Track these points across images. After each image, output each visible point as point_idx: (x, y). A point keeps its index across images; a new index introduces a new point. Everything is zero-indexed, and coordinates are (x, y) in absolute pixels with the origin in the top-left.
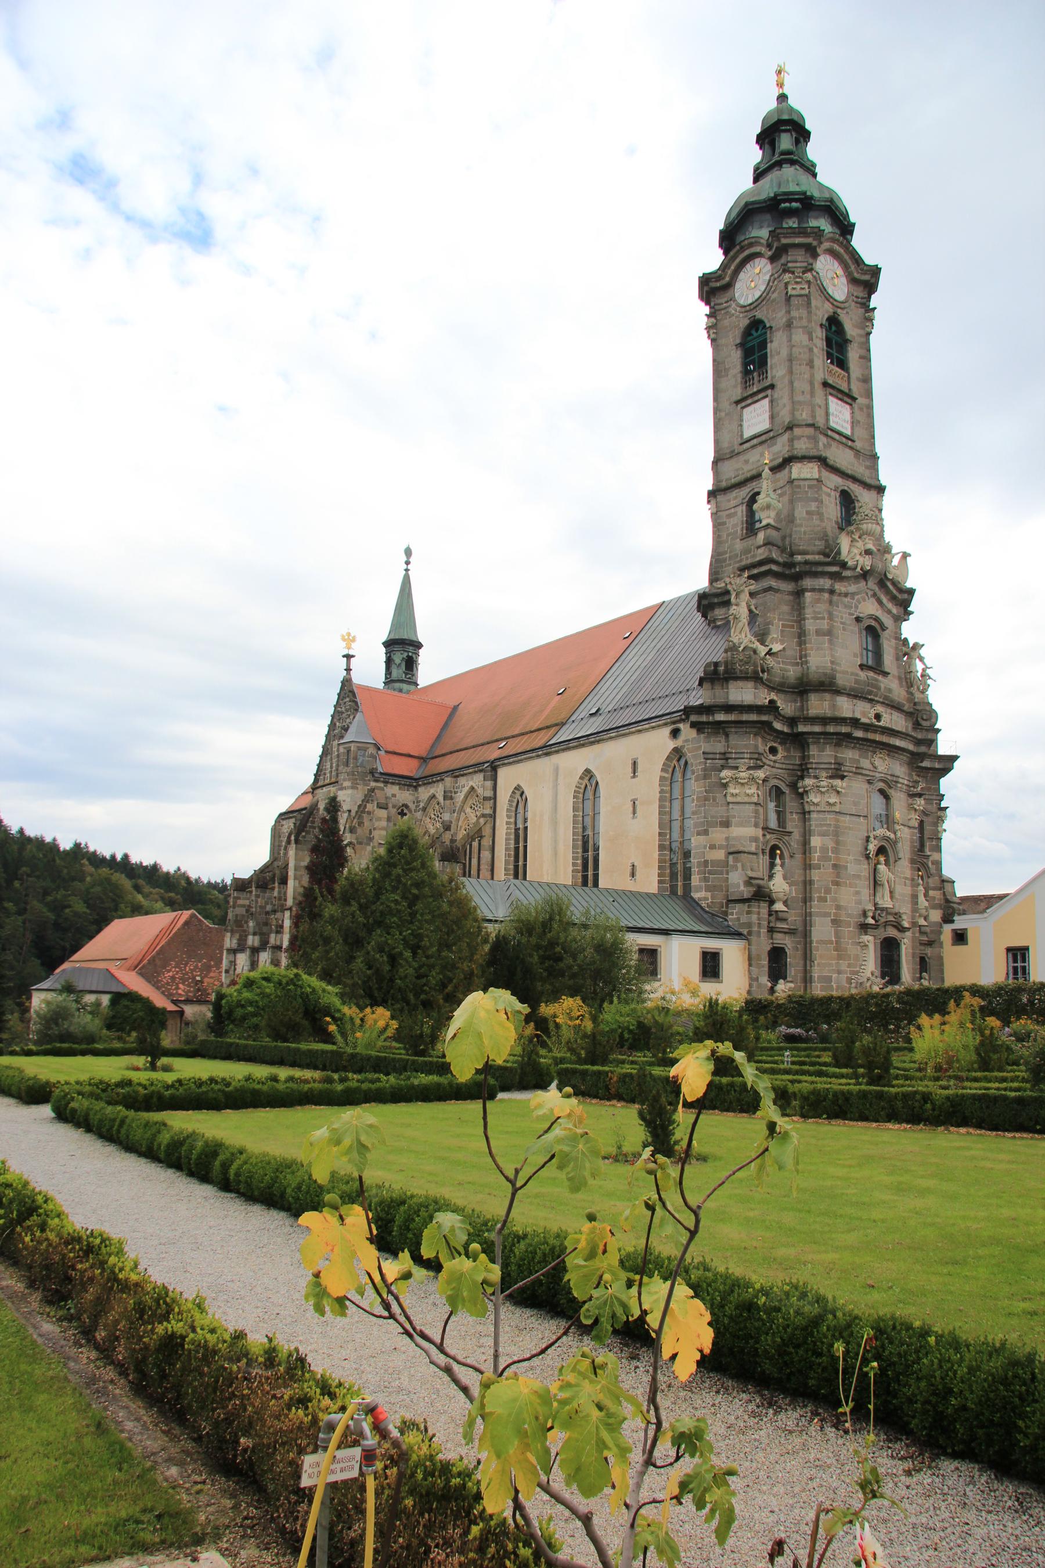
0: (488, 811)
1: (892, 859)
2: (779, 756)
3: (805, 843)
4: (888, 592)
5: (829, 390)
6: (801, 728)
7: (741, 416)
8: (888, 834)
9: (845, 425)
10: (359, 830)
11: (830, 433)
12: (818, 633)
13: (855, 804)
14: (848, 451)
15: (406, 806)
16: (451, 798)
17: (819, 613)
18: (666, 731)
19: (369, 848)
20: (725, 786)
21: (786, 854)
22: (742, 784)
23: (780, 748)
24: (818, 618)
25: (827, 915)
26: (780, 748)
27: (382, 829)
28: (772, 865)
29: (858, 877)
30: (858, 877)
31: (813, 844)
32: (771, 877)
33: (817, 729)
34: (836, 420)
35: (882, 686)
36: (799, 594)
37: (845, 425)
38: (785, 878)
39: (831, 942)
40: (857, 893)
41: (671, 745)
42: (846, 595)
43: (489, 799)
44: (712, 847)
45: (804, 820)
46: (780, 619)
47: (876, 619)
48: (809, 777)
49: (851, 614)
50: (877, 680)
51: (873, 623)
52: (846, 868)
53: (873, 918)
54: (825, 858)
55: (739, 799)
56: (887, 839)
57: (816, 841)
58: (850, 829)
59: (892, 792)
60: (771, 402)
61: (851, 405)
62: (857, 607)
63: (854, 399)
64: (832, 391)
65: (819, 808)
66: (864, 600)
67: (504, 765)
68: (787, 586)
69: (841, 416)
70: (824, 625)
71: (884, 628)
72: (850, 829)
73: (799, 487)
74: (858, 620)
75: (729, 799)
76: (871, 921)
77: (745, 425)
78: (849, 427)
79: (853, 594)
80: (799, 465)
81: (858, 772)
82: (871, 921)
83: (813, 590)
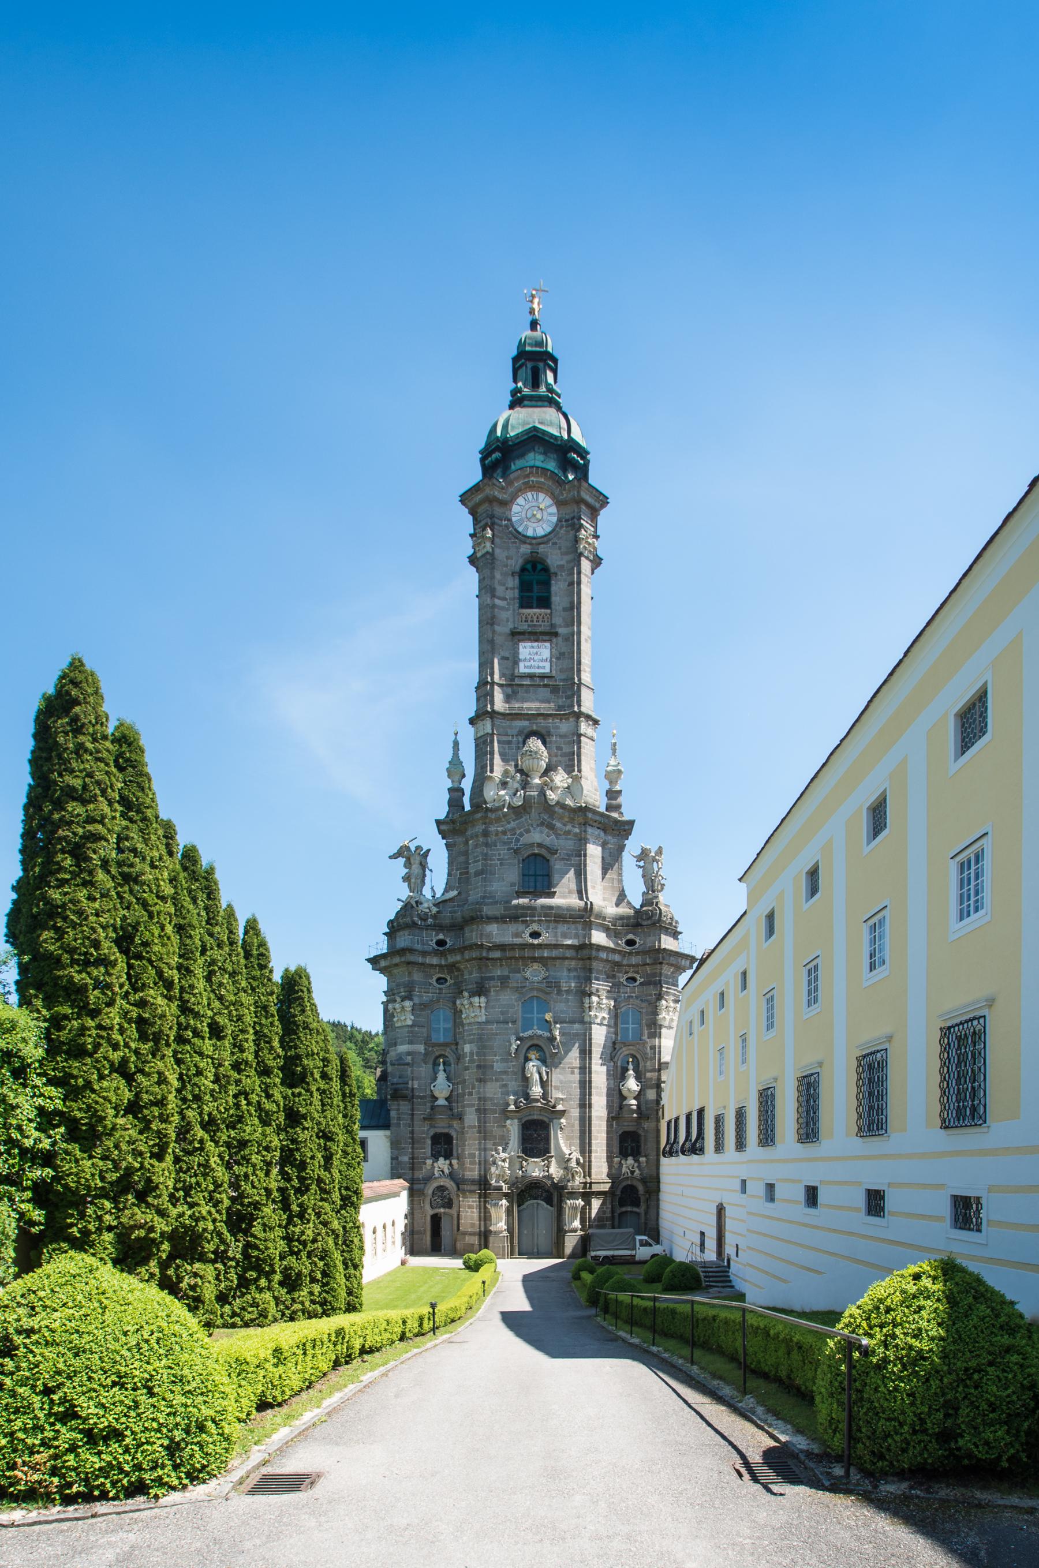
4: (561, 818)
5: (517, 637)
9: (541, 664)
11: (517, 681)
12: (477, 874)
13: (502, 1013)
25: (473, 1105)
29: (505, 1073)
30: (505, 1073)
33: (458, 958)
34: (528, 664)
37: (541, 664)
39: (475, 1127)
52: (492, 1066)
54: (472, 1061)
57: (467, 1048)
58: (497, 1034)
62: (518, 840)
63: (556, 634)
64: (522, 637)
69: (536, 657)
70: (479, 866)
72: (497, 1034)
76: (512, 1107)
83: (472, 838)
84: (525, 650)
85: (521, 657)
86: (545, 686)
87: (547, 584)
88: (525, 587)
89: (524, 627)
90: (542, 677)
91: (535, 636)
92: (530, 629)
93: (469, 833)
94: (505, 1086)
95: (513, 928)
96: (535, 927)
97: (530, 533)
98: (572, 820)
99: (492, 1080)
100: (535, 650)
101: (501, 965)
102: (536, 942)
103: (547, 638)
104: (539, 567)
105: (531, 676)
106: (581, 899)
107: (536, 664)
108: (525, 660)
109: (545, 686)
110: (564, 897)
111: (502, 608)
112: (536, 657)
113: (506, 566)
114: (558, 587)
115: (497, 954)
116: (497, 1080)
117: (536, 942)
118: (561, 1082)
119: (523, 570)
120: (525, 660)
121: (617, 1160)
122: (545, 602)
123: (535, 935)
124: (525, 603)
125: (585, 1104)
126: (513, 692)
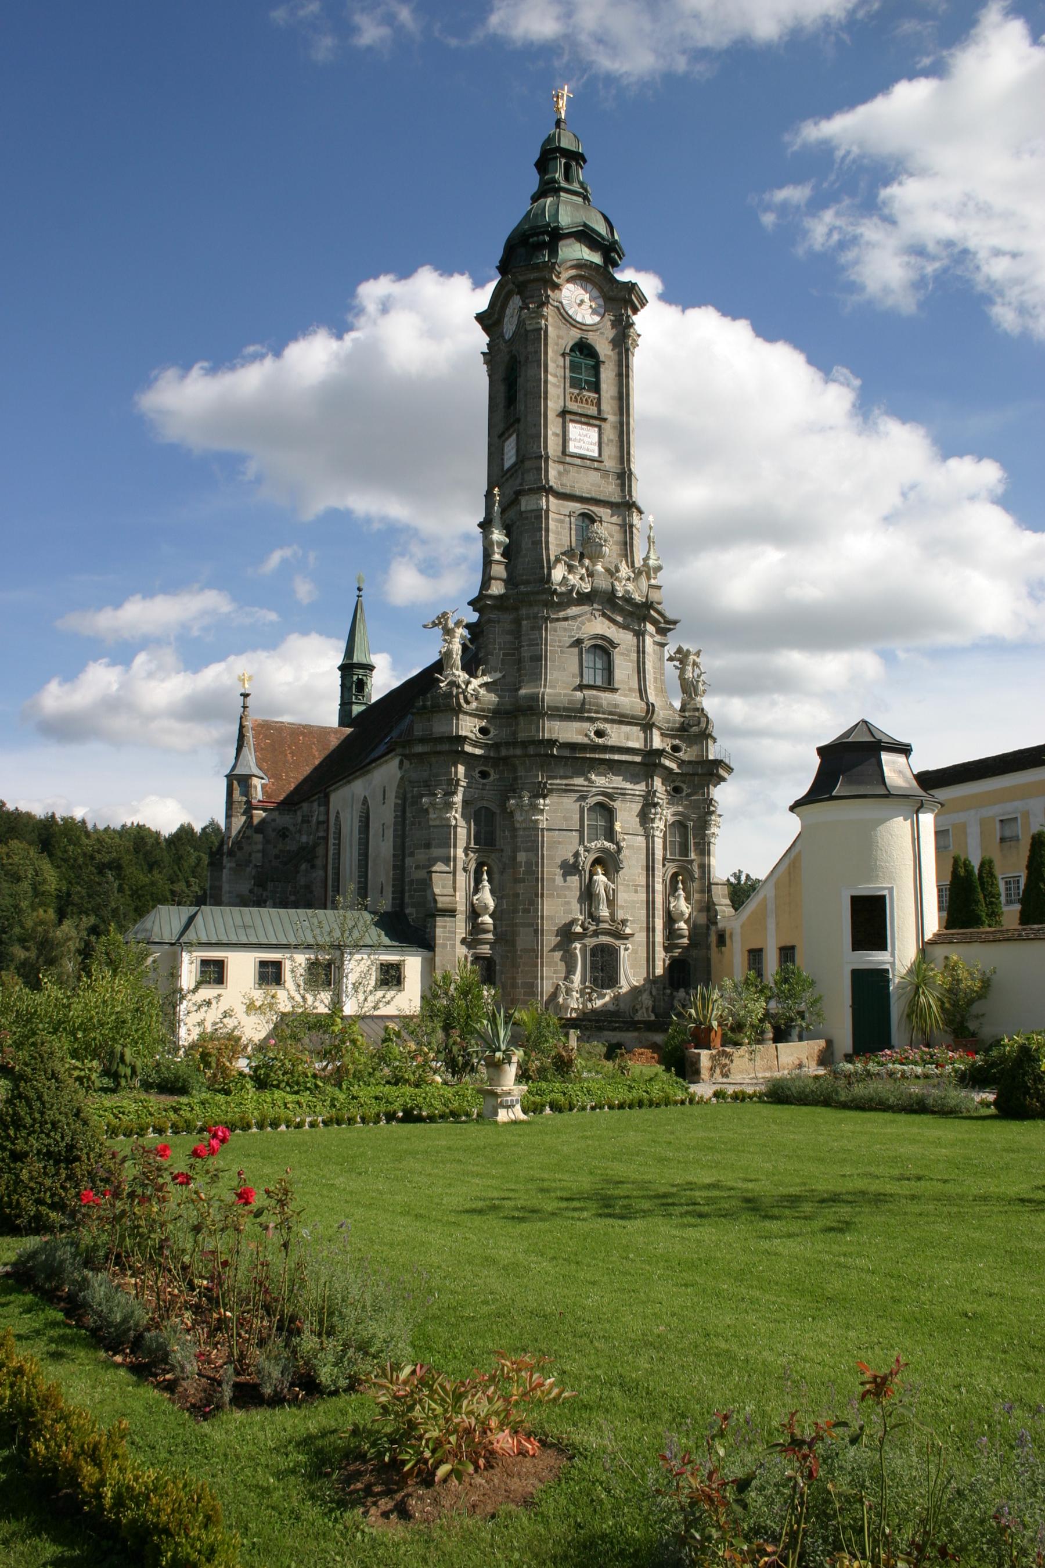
0: (321, 834)
1: (611, 870)
2: (492, 778)
3: (514, 858)
4: (621, 611)
6: (504, 752)
7: (503, 446)
8: (607, 844)
10: (239, 854)
11: (568, 459)
13: (565, 819)
14: (592, 472)
15: (287, 829)
16: (309, 822)
17: (533, 640)
18: (396, 762)
19: (248, 869)
20: (427, 811)
21: (495, 869)
22: (440, 809)
23: (492, 772)
24: (533, 645)
26: (492, 772)
27: (258, 851)
28: (478, 881)
31: (519, 859)
32: (477, 890)
35: (604, 703)
36: (518, 622)
38: (492, 892)
40: (568, 903)
41: (399, 775)
42: (566, 619)
43: (323, 822)
44: (417, 867)
45: (514, 837)
46: (500, 649)
47: (603, 638)
48: (514, 798)
49: (571, 637)
50: (596, 697)
51: (600, 642)
53: (582, 926)
55: (437, 823)
56: (605, 850)
58: (559, 843)
59: (617, 805)
60: (518, 436)
61: (599, 427)
63: (605, 420)
64: (573, 417)
65: (524, 825)
66: (590, 621)
67: (334, 790)
68: (508, 617)
71: (614, 645)
72: (559, 843)
73: (527, 518)
74: (578, 642)
75: (431, 823)
76: (579, 929)
77: (506, 457)
78: (596, 448)
79: (574, 618)
80: (527, 497)
81: (567, 790)
82: (579, 929)
84: (575, 430)
85: (571, 436)
86: (595, 469)
87: (596, 369)
88: (574, 367)
89: (573, 406)
90: (592, 460)
91: (586, 419)
92: (580, 411)
93: (523, 612)
94: (568, 903)
95: (576, 725)
96: (601, 725)
97: (579, 319)
98: (631, 614)
99: (551, 896)
100: (585, 432)
101: (566, 765)
102: (600, 741)
103: (597, 422)
104: (585, 352)
105: (582, 457)
106: (641, 698)
107: (586, 446)
108: (575, 440)
109: (595, 469)
110: (625, 696)
111: (554, 385)
112: (586, 439)
113: (557, 344)
114: (607, 376)
115: (566, 753)
116: (559, 897)
117: (600, 741)
118: (626, 901)
119: (572, 350)
120: (575, 440)
121: (668, 991)
122: (596, 387)
123: (600, 734)
124: (575, 383)
125: (650, 929)
126: (565, 470)
